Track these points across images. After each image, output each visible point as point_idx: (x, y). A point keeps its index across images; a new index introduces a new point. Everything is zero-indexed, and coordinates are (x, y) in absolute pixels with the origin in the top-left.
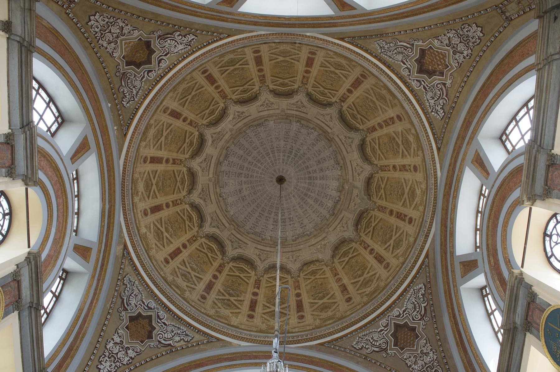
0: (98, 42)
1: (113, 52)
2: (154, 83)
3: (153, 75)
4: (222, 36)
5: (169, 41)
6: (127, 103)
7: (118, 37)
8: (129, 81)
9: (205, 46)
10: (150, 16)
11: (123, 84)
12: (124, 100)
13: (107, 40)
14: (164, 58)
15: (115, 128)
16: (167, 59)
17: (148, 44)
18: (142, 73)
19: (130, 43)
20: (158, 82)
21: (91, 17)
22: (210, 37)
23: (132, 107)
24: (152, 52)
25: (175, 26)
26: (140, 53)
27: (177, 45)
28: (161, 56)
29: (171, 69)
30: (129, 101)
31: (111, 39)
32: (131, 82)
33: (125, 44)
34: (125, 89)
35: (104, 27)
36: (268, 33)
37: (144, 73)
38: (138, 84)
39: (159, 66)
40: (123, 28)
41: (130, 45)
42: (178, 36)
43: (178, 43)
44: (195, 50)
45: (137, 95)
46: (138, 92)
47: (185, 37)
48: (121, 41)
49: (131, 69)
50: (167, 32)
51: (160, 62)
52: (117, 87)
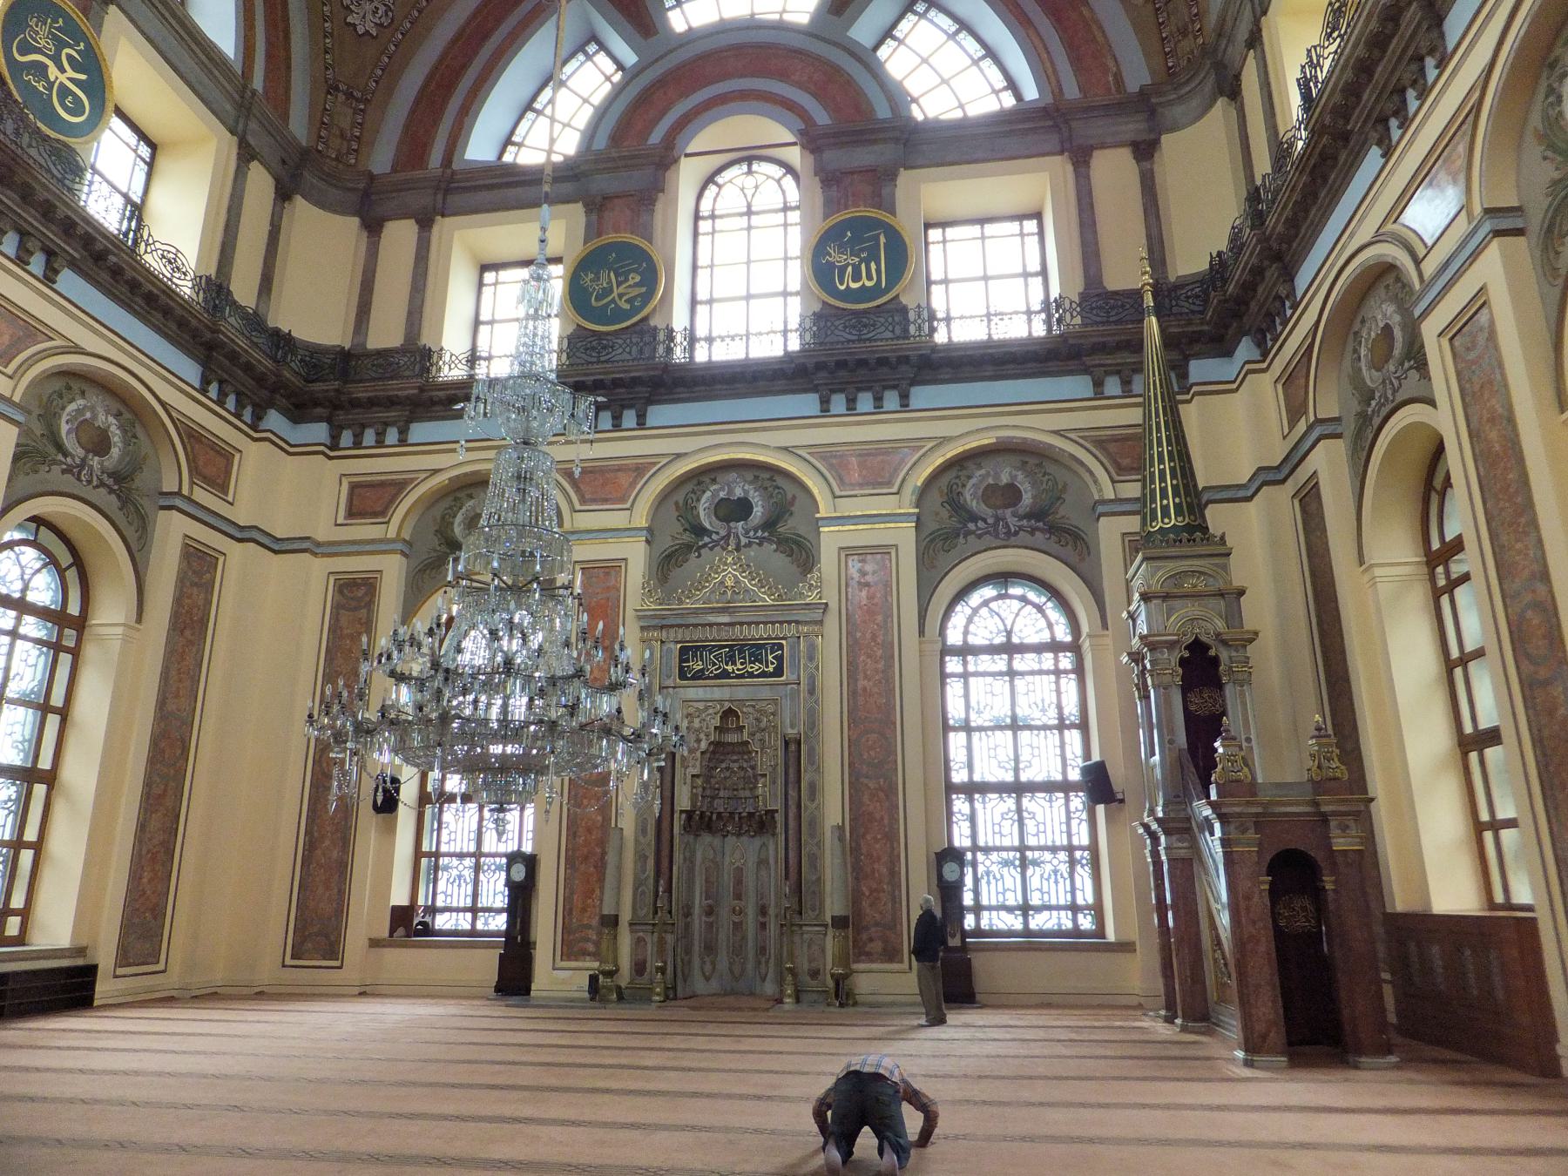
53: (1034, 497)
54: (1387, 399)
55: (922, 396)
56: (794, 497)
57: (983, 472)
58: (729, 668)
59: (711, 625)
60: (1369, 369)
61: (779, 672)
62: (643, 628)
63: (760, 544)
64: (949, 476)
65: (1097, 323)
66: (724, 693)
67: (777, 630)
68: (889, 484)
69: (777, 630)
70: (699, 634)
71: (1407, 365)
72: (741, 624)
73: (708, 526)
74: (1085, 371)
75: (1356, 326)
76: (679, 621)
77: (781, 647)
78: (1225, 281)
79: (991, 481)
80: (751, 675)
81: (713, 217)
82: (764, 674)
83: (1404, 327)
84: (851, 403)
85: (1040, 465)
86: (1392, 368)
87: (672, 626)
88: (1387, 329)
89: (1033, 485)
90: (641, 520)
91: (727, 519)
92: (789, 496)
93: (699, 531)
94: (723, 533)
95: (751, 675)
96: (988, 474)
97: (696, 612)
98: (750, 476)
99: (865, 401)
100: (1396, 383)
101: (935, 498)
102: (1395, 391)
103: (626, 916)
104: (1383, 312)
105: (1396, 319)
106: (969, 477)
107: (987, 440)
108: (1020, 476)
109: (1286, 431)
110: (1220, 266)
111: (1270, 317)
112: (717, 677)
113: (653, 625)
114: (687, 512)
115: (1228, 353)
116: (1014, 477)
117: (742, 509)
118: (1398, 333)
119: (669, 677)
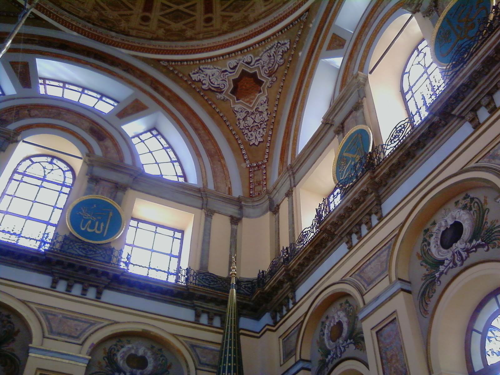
0: (268, 120)
1: (265, 102)
2: (251, 48)
3: (247, 58)
4: (166, 64)
5: (216, 84)
6: (285, 44)
7: (253, 113)
8: (270, 65)
9: (187, 61)
10: (217, 116)
11: (277, 65)
12: (286, 49)
13: (261, 116)
14: (229, 70)
15: (311, 25)
16: (226, 66)
17: (234, 92)
18: (256, 66)
19: (247, 102)
20: (246, 48)
21: (257, 144)
22: (177, 68)
23: (285, 37)
24: (235, 82)
25: (202, 96)
26: (246, 86)
27: (211, 75)
28: (230, 73)
29: (229, 54)
30: (283, 45)
31: (258, 115)
32: (269, 63)
33: (251, 103)
34: (278, 60)
35: (255, 129)
36: (118, 49)
37: (254, 65)
38: (265, 58)
39: (238, 64)
40: (243, 119)
41: (248, 99)
42: (205, 84)
43: (209, 77)
44: (198, 62)
45: (273, 47)
46: (270, 49)
47: (200, 80)
48: (252, 108)
49: (262, 76)
50: (212, 94)
51: (235, 68)
52: (283, 67)
53: (155, 367)
54: (337, 356)
55: (109, 296)
56: (18, 331)
57: (130, 346)
60: (329, 340)
64: (114, 342)
65: (204, 286)
68: (77, 338)
71: (349, 341)
74: (193, 307)
75: (323, 319)
78: (264, 284)
79: (133, 352)
81: (24, 174)
83: (349, 323)
84: (69, 288)
85: (160, 350)
86: (341, 341)
88: (340, 324)
89: (155, 360)
96: (133, 348)
99: (77, 289)
100: (342, 349)
101: (101, 355)
102: (341, 353)
104: (338, 315)
105: (344, 320)
106: (122, 347)
107: (138, 328)
108: (149, 353)
109: (282, 363)
110: (262, 278)
111: (281, 305)
115: (258, 318)
116: (145, 353)
118: (345, 326)
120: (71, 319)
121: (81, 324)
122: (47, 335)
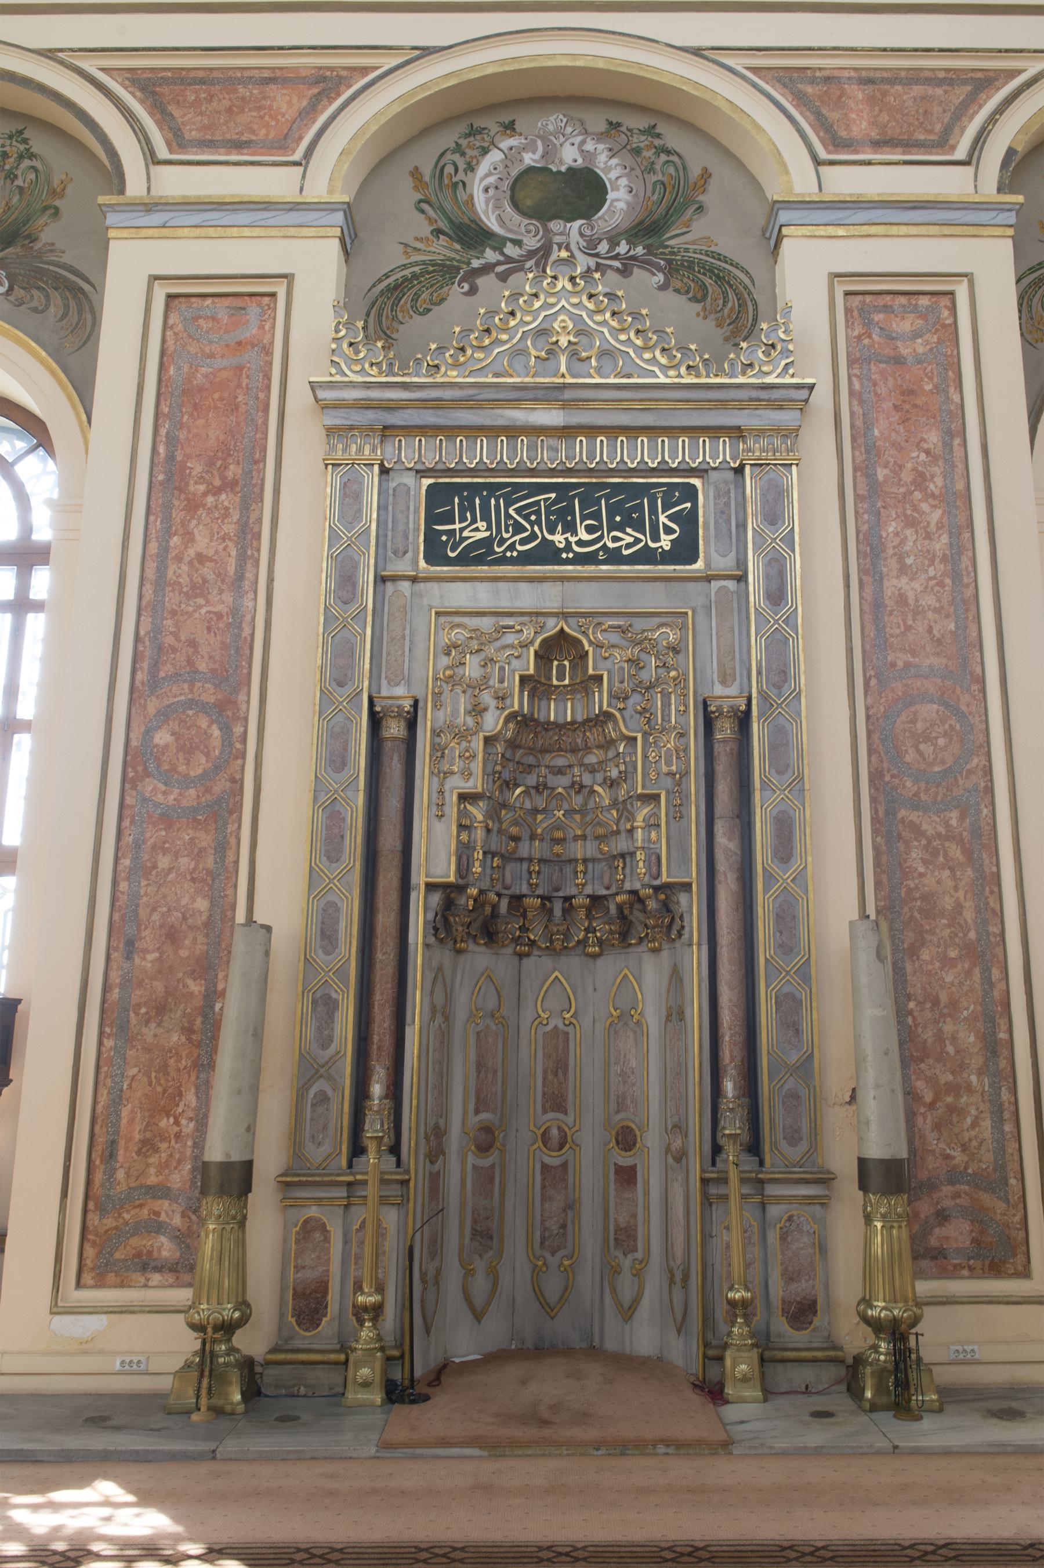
58: (558, 539)
59: (513, 432)
61: (685, 550)
62: (331, 431)
63: (625, 272)
66: (547, 597)
67: (679, 452)
69: (679, 452)
70: (481, 453)
72: (592, 431)
73: (494, 226)
76: (429, 418)
77: (690, 493)
80: (614, 557)
82: (647, 556)
87: (409, 430)
90: (328, 173)
91: (542, 213)
92: (695, 171)
93: (473, 235)
94: (532, 243)
95: (614, 557)
97: (474, 399)
98: (597, 121)
103: (269, 1163)
112: (525, 559)
113: (364, 422)
114: (441, 189)
117: (583, 191)
119: (400, 553)
120: (893, 81)
121: (939, 91)
122: (823, 154)
